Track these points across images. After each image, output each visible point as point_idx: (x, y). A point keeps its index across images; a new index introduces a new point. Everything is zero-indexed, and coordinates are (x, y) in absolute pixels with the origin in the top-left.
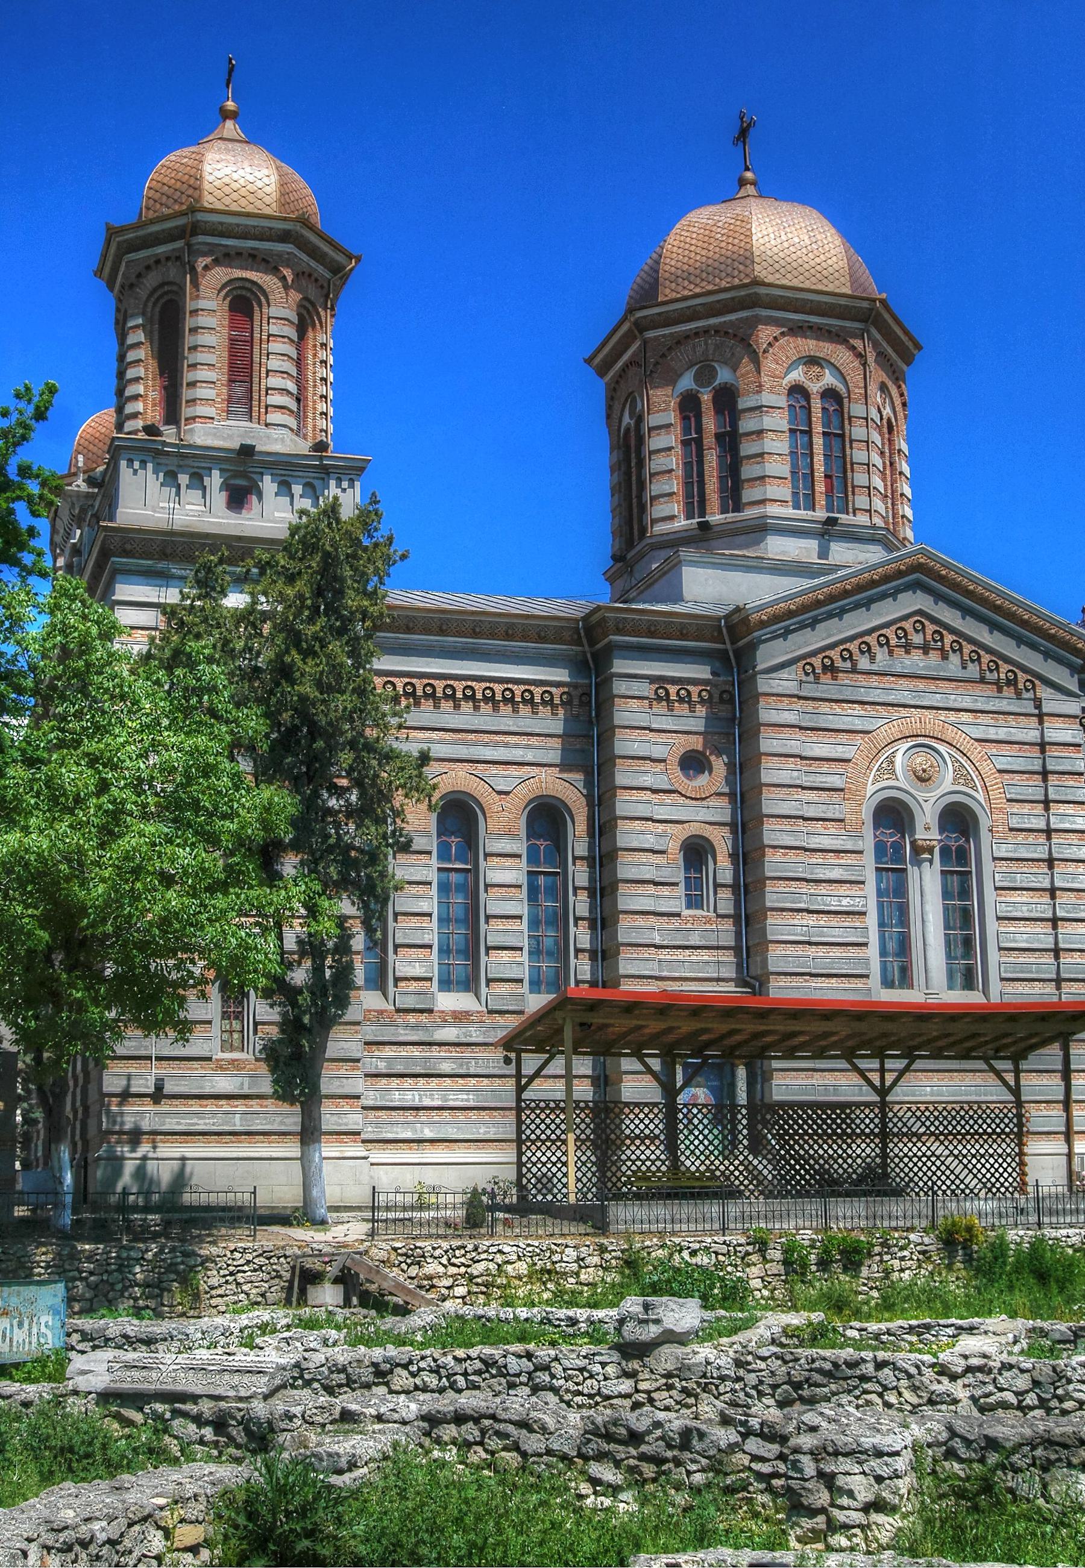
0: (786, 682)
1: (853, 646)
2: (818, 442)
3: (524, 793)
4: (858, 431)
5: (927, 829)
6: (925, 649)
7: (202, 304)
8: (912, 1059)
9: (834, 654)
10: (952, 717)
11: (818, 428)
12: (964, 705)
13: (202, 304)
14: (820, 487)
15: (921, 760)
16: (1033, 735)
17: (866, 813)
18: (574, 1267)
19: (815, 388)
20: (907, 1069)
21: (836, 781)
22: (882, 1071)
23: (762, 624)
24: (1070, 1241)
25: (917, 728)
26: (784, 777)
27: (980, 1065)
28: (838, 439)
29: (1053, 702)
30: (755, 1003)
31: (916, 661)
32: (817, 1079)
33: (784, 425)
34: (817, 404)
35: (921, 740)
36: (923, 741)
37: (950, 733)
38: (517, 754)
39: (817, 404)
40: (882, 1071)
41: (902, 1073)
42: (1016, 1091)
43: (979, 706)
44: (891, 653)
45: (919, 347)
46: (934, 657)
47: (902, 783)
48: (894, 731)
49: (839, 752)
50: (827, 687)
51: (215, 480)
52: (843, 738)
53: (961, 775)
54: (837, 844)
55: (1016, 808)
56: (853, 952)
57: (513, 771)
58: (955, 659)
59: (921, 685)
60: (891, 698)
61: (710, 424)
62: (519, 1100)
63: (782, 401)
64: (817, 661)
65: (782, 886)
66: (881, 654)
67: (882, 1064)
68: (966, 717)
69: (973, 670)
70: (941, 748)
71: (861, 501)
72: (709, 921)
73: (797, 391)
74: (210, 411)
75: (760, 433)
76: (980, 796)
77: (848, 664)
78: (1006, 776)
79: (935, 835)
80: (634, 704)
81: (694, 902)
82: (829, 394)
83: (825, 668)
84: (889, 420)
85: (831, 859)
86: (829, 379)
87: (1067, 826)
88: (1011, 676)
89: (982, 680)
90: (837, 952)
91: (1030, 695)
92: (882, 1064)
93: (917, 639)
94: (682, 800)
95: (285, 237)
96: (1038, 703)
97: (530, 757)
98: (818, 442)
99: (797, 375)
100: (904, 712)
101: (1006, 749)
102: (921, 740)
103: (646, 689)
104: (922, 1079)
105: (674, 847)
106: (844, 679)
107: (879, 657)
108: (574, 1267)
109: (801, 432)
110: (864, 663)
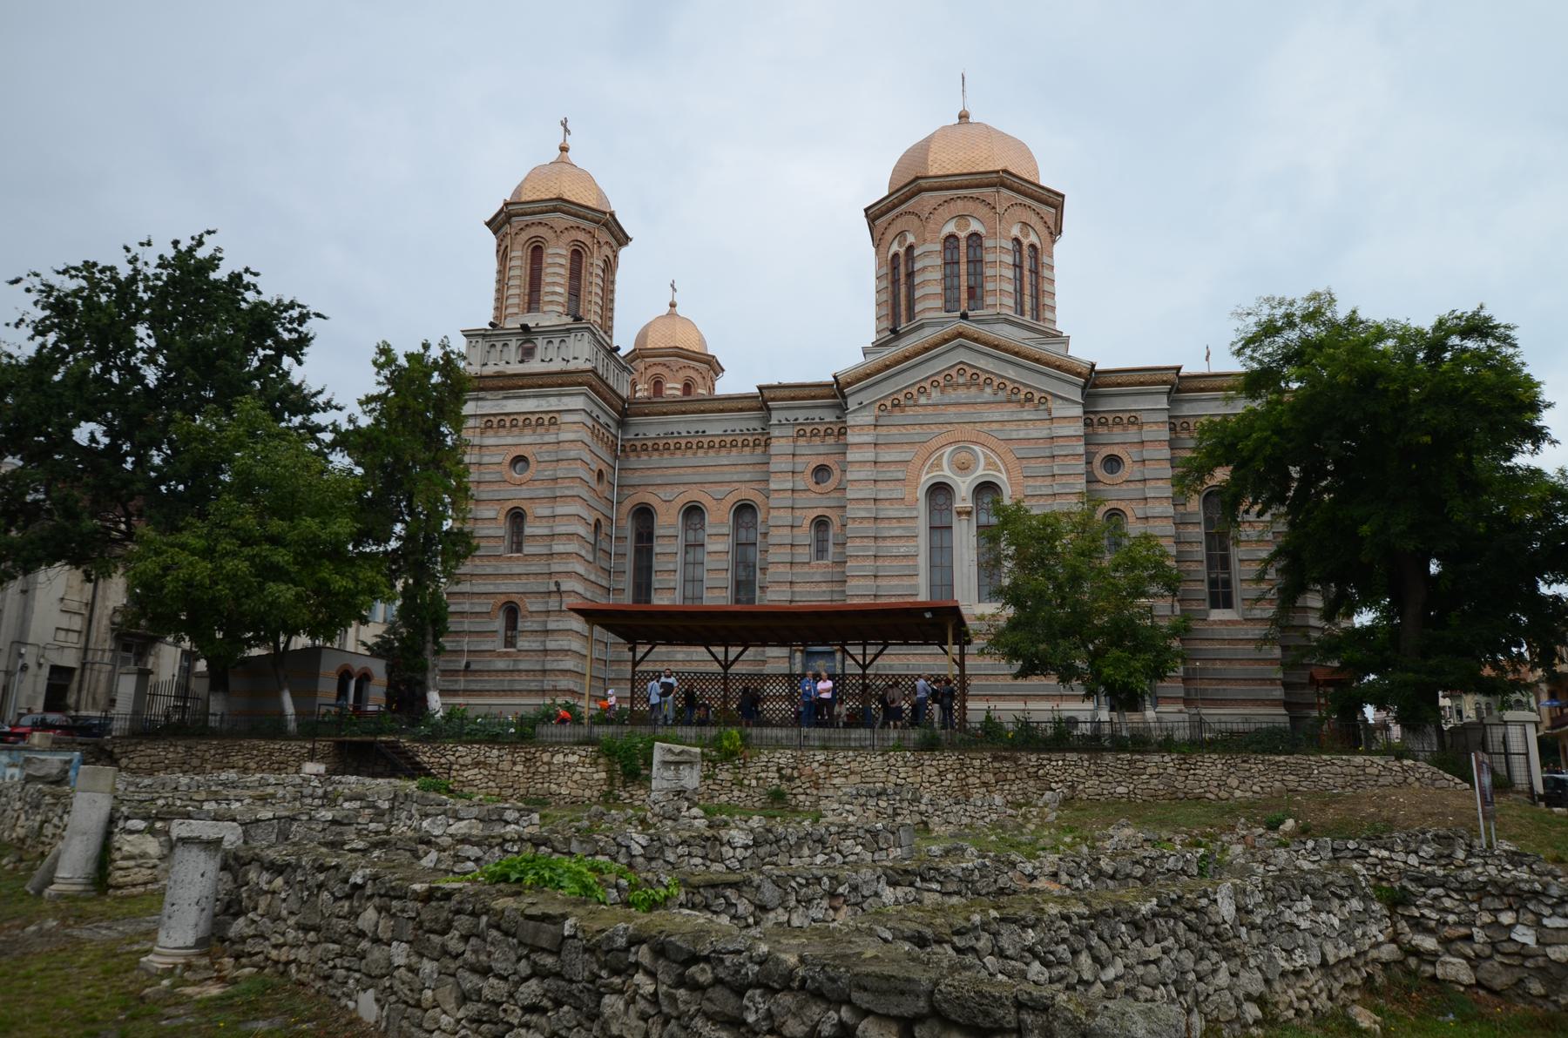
0: (866, 417)
1: (914, 390)
2: (963, 267)
3: (732, 499)
4: (988, 257)
5: (964, 500)
6: (967, 386)
7: (513, 254)
8: (886, 646)
9: (901, 397)
10: (985, 427)
11: (963, 260)
12: (995, 419)
13: (513, 254)
14: (964, 296)
15: (963, 456)
16: (1045, 433)
17: (921, 493)
18: (496, 761)
19: (962, 235)
20: (880, 653)
21: (900, 476)
22: (864, 655)
23: (849, 384)
24: (817, 758)
25: (958, 436)
26: (862, 476)
27: (937, 649)
28: (976, 262)
29: (1059, 409)
30: (642, 607)
31: (962, 394)
32: (913, 661)
33: (939, 261)
34: (963, 245)
35: (961, 444)
36: (961, 445)
37: (982, 438)
38: (727, 478)
39: (963, 245)
40: (864, 655)
41: (876, 656)
42: (962, 665)
43: (1006, 418)
44: (942, 392)
45: (1063, 196)
46: (973, 390)
47: (947, 472)
48: (942, 440)
49: (903, 457)
50: (898, 417)
51: (514, 344)
52: (906, 448)
53: (990, 464)
54: (898, 514)
55: (1031, 482)
56: (906, 582)
57: (727, 488)
58: (988, 390)
59: (964, 409)
60: (941, 420)
61: (902, 269)
62: (634, 673)
63: (938, 247)
64: (889, 403)
65: (858, 542)
66: (935, 395)
67: (864, 650)
68: (995, 426)
69: (1002, 395)
70: (976, 448)
71: (989, 300)
72: (827, 566)
73: (952, 237)
74: (516, 310)
75: (924, 269)
76: (1004, 477)
77: (911, 402)
78: (1025, 462)
79: (969, 504)
80: (783, 441)
81: (821, 552)
82: (975, 236)
83: (894, 406)
84: (1033, 246)
85: (895, 524)
86: (975, 226)
87: (1068, 491)
88: (1029, 396)
89: (1009, 401)
90: (895, 582)
91: (1042, 407)
92: (864, 650)
93: (961, 380)
94: (813, 495)
95: (555, 210)
96: (1049, 411)
97: (735, 478)
98: (963, 267)
99: (950, 228)
100: (949, 427)
101: (1025, 445)
102: (961, 444)
103: (791, 431)
104: (895, 661)
105: (807, 523)
106: (909, 411)
107: (933, 395)
108: (496, 761)
109: (951, 263)
110: (923, 400)
